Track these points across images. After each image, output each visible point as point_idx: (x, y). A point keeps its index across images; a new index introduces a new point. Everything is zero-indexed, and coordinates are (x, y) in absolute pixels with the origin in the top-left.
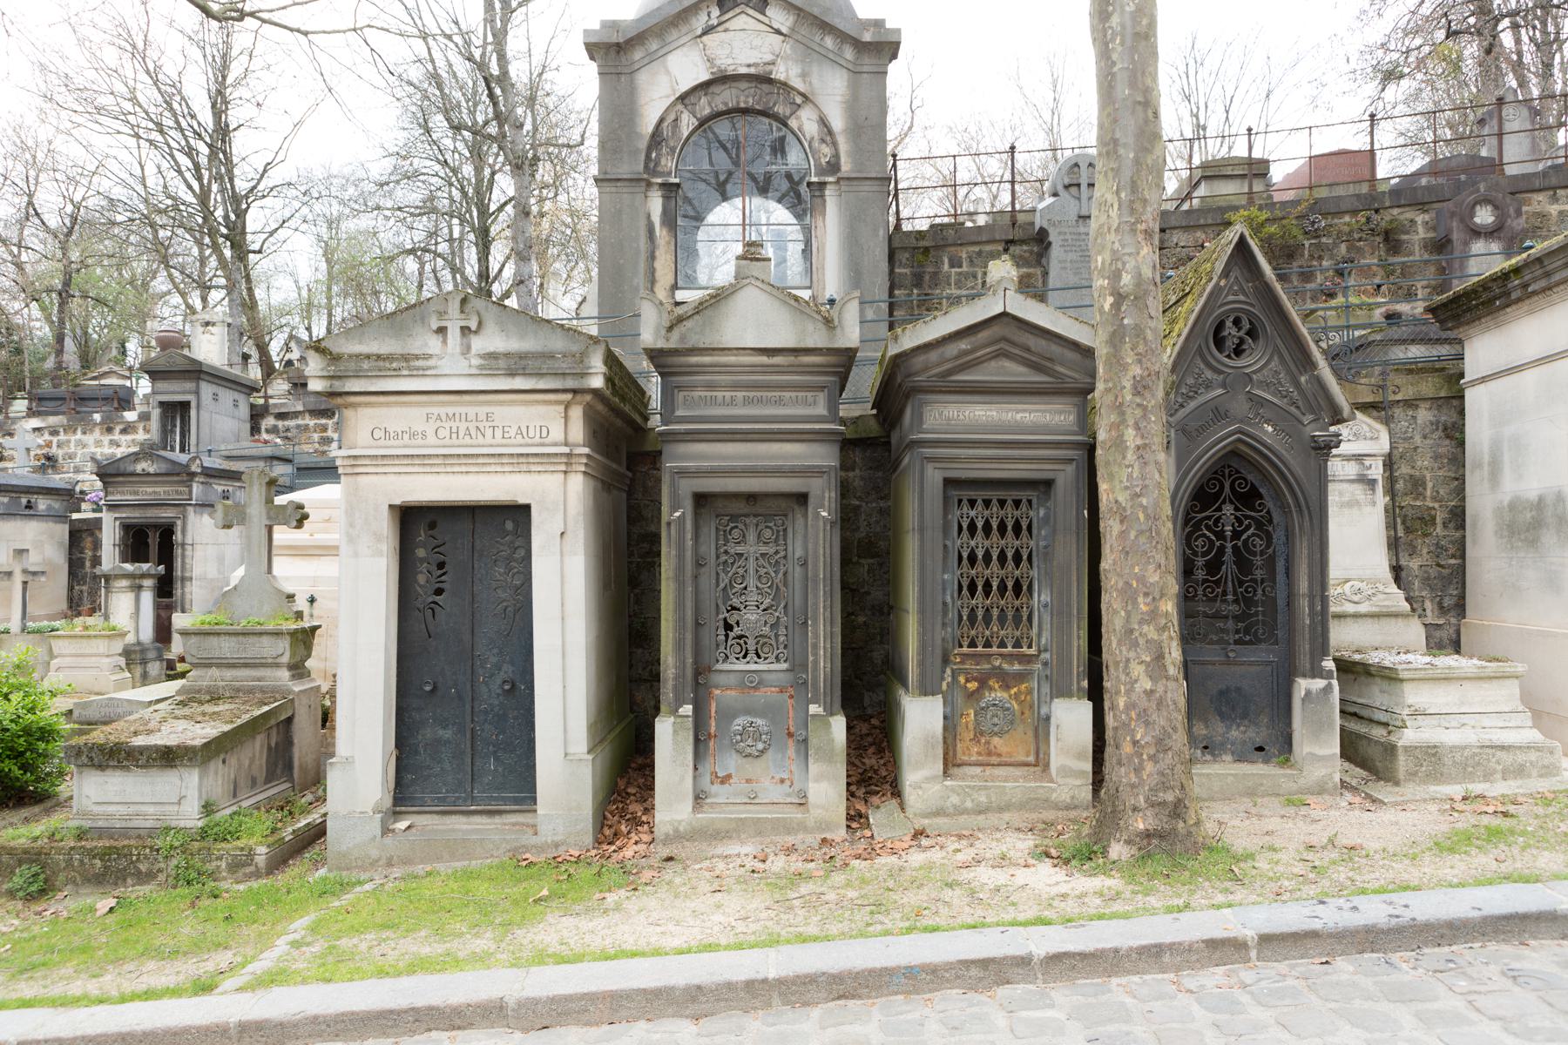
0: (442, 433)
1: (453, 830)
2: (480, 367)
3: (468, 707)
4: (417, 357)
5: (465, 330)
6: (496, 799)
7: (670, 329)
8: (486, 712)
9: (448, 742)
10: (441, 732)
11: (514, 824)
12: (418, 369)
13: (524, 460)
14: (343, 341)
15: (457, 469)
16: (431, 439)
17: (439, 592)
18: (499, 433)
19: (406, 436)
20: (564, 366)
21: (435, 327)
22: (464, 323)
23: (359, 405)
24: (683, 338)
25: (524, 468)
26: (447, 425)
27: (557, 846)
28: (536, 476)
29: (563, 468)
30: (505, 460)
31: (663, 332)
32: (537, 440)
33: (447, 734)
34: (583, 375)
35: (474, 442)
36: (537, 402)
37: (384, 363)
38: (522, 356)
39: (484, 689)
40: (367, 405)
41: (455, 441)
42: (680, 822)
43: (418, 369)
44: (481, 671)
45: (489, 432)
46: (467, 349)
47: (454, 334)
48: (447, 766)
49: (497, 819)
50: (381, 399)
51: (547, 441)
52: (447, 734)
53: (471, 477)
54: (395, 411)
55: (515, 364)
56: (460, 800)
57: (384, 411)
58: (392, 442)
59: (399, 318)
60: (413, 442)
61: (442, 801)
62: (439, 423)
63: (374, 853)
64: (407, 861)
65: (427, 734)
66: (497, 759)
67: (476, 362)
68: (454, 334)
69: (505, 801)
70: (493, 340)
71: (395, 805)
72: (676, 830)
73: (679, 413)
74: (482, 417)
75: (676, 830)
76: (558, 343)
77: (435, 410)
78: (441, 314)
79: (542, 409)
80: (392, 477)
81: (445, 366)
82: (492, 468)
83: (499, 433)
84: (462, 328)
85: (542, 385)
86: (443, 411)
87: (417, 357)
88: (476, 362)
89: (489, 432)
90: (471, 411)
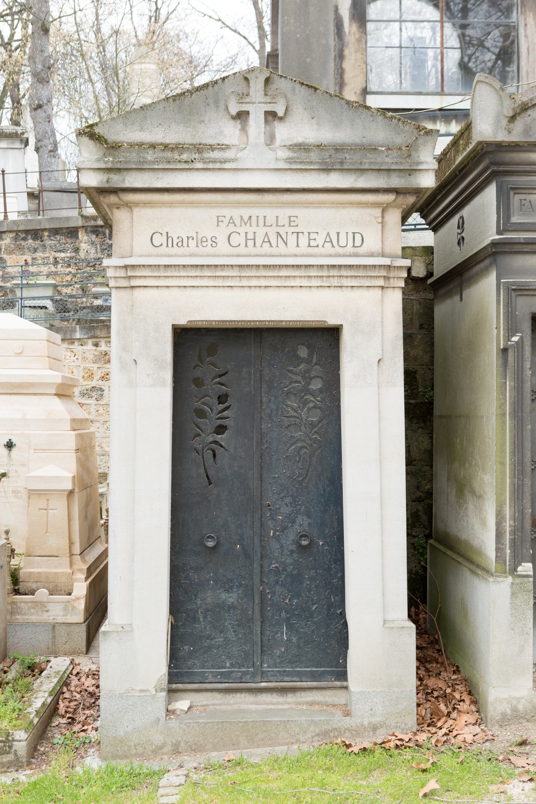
0: (236, 239)
1: (244, 711)
2: (289, 160)
3: (256, 565)
4: (212, 148)
5: (271, 116)
6: (288, 674)
7: (512, 119)
8: (277, 572)
9: (232, 607)
10: (224, 596)
11: (312, 704)
12: (214, 161)
13: (336, 272)
14: (119, 126)
15: (254, 282)
16: (223, 247)
17: (221, 429)
18: (303, 240)
19: (192, 243)
20: (389, 160)
21: (234, 112)
22: (269, 108)
23: (137, 204)
24: (527, 131)
25: (335, 282)
26: (242, 230)
27: (375, 729)
28: (349, 293)
29: (381, 282)
30: (313, 272)
31: (505, 122)
32: (350, 249)
33: (231, 598)
34: (411, 172)
35: (275, 251)
36: (351, 204)
37: (172, 154)
38: (339, 148)
39: (274, 545)
40: (146, 204)
41: (251, 249)
42: (518, 700)
43: (214, 161)
44: (270, 523)
45: (292, 240)
46: (271, 139)
47: (257, 121)
48: (231, 635)
49: (291, 698)
50: (166, 197)
51: (361, 250)
52: (231, 598)
53: (271, 294)
54: (178, 212)
55: (332, 158)
56: (244, 673)
57: (165, 212)
58: (176, 250)
59: (187, 100)
60: (201, 250)
61: (226, 677)
62: (231, 228)
63: (157, 738)
64: (196, 749)
65: (209, 597)
66: (290, 627)
67: (284, 154)
68: (257, 121)
69: (301, 676)
70: (302, 128)
71: (170, 682)
72: (515, 710)
73: (515, 219)
74: (283, 220)
75: (515, 710)
76: (379, 133)
77: (227, 212)
78: (242, 97)
79: (355, 213)
80: (176, 291)
81: (247, 158)
82: (297, 282)
83: (303, 240)
84: (267, 113)
85: (362, 182)
86: (236, 213)
87: (212, 148)
88: (284, 154)
89: (292, 240)
90: (271, 214)
